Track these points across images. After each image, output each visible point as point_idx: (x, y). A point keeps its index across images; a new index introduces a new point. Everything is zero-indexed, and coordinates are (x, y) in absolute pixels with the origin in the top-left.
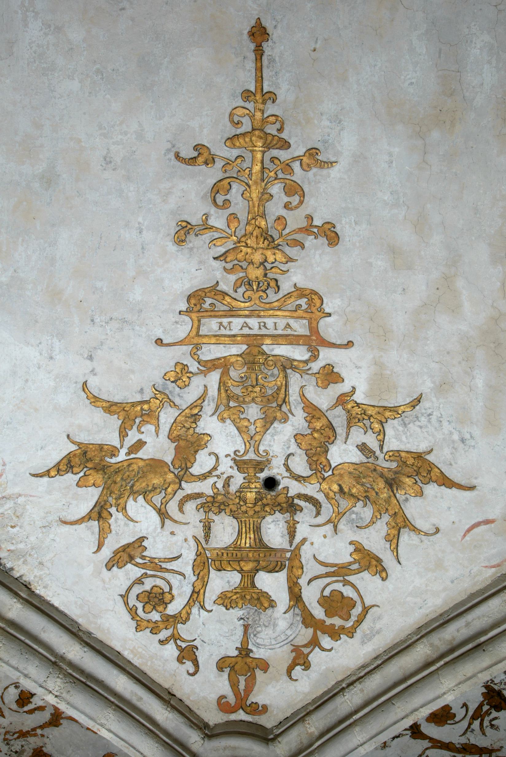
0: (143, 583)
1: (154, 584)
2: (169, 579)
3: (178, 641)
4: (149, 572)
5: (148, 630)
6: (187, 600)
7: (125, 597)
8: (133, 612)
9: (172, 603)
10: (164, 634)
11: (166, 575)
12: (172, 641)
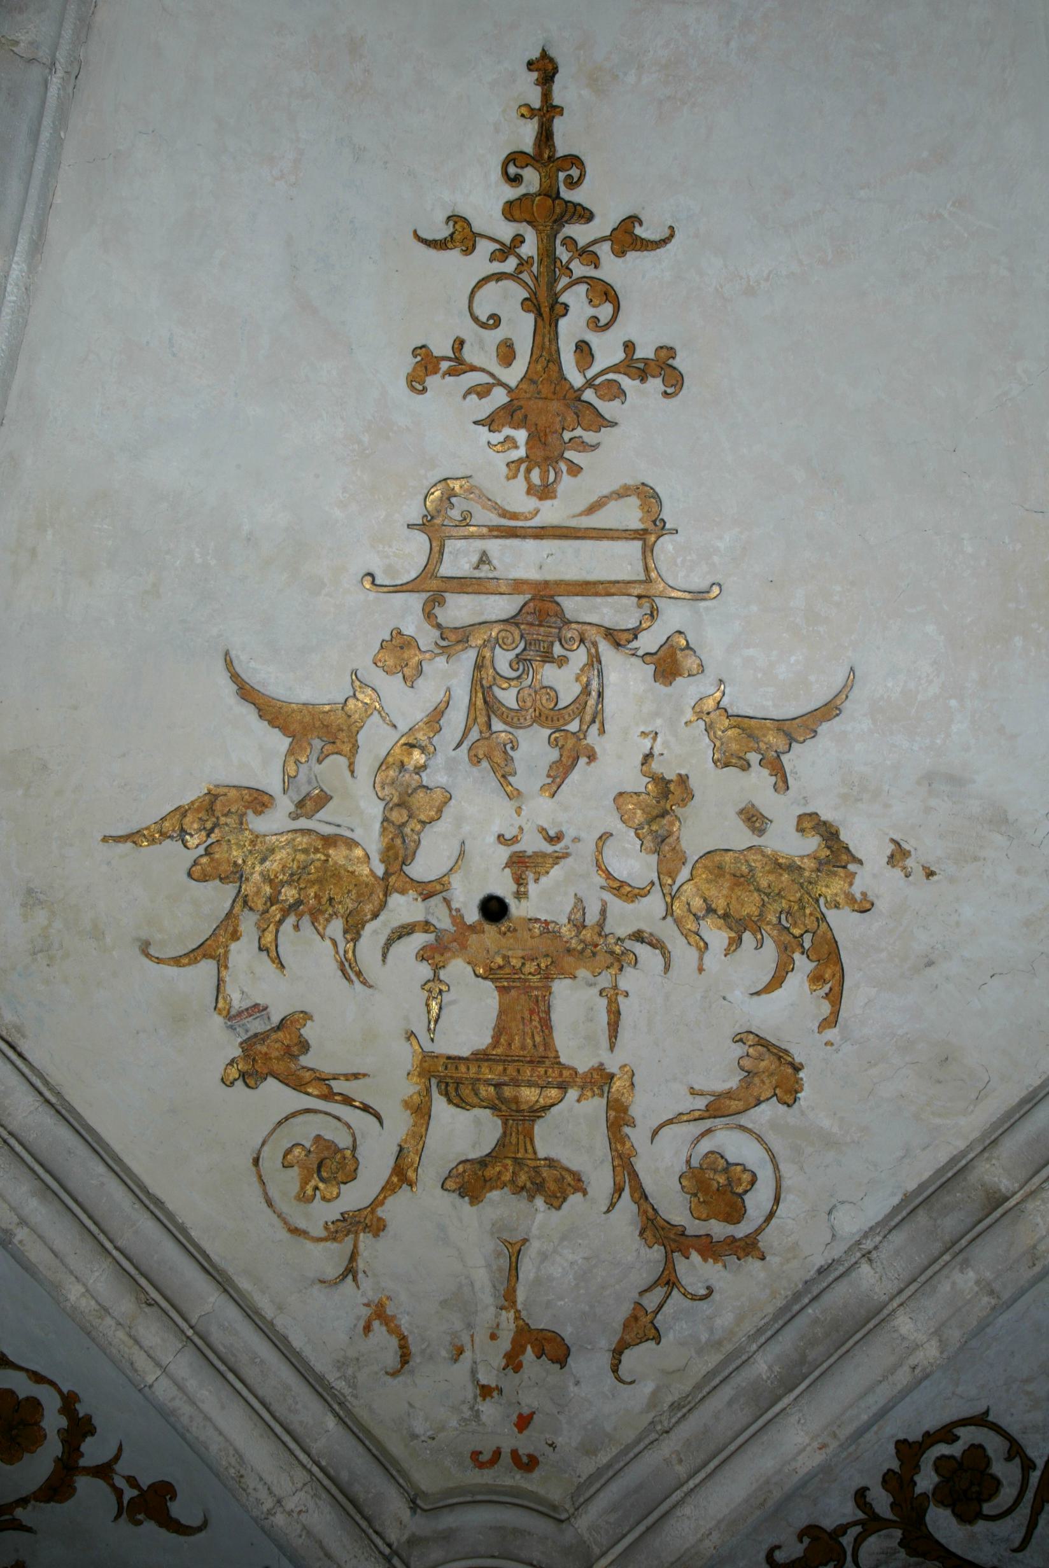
0: (1009, 1458)
1: (1005, 1482)
2: (1014, 1515)
3: (858, 1529)
4: (1035, 1476)
5: (895, 1465)
6: (959, 1552)
7: (981, 1420)
8: (947, 1433)
9: (954, 1520)
10: (881, 1501)
11: (1025, 1510)
12: (861, 1515)
